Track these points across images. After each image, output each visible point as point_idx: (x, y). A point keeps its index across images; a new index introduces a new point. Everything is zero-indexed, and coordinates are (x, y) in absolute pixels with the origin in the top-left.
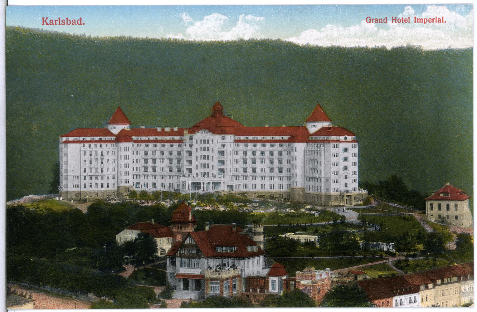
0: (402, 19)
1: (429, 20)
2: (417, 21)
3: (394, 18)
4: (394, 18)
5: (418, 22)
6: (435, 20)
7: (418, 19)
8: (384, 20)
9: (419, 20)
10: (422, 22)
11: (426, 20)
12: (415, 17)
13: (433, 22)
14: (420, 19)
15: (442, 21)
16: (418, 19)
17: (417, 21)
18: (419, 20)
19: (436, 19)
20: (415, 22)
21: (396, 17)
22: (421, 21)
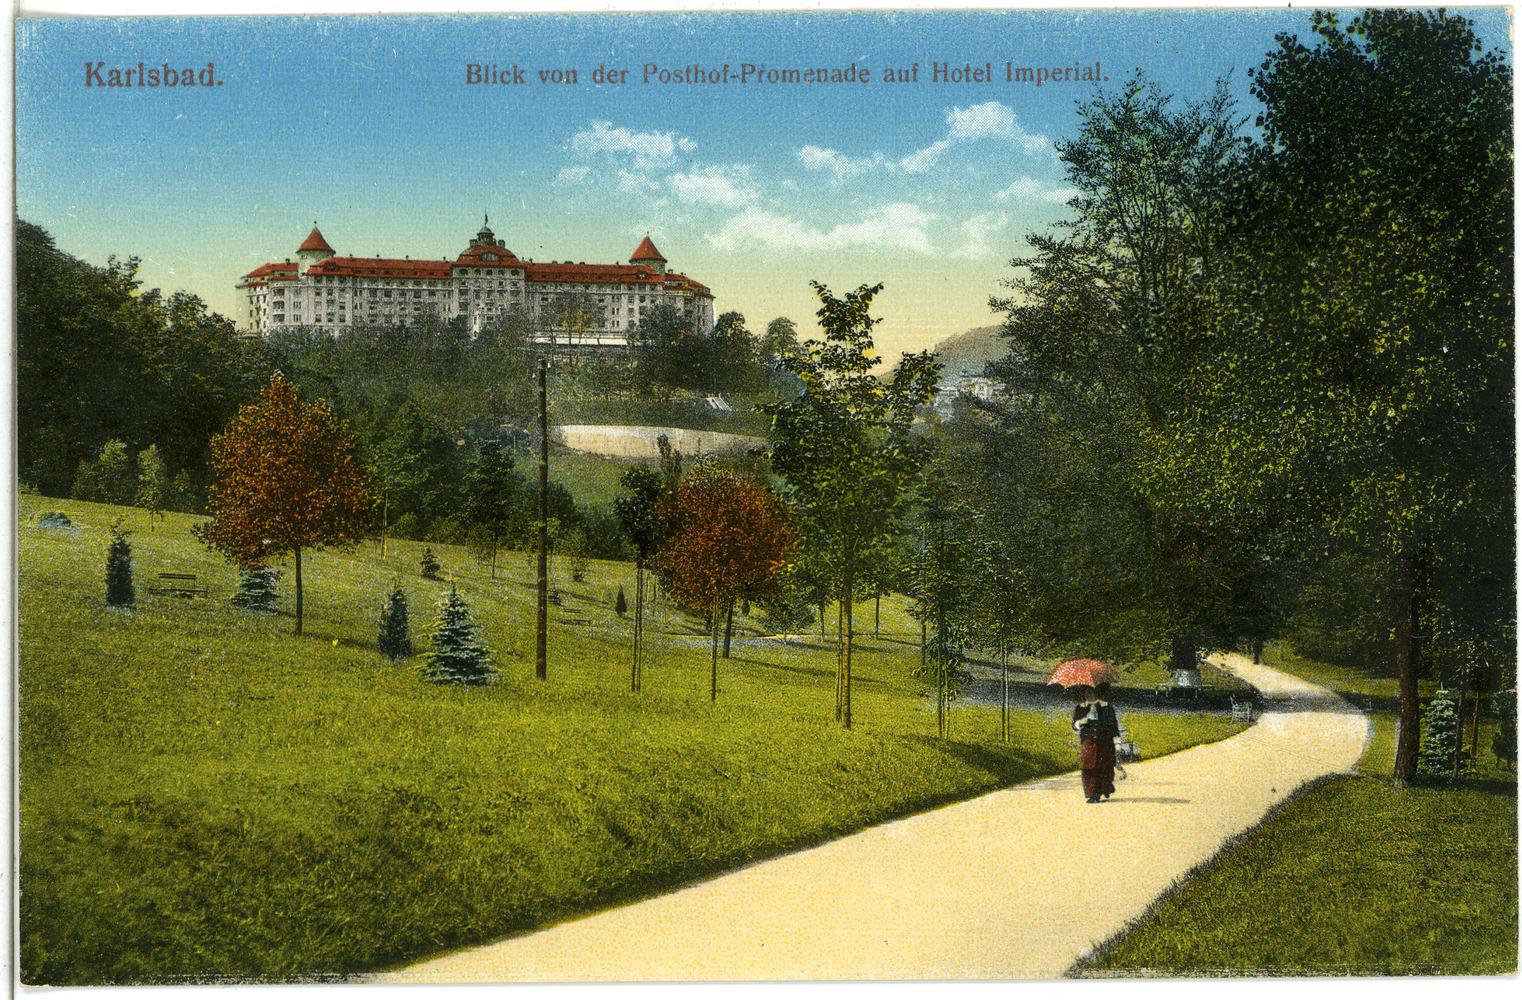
1: (1054, 73)
2: (1014, 73)
3: (940, 67)
4: (940, 67)
6: (1072, 75)
7: (1018, 71)
13: (1067, 79)
16: (1018, 71)
17: (1014, 76)
20: (1009, 79)
21: (946, 65)
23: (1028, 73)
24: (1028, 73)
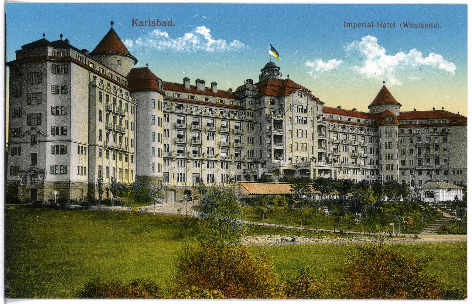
0: (388, 24)
1: (358, 25)
2: (346, 24)
4: (380, 23)
5: (347, 27)
6: (364, 25)
7: (347, 24)
8: (168, 24)
9: (348, 25)
10: (352, 27)
11: (355, 25)
12: (345, 22)
13: (363, 27)
14: (350, 24)
15: (371, 26)
16: (347, 24)
17: (346, 26)
18: (348, 25)
19: (366, 24)
20: (345, 27)
22: (351, 26)
23: (351, 25)
24: (351, 25)
